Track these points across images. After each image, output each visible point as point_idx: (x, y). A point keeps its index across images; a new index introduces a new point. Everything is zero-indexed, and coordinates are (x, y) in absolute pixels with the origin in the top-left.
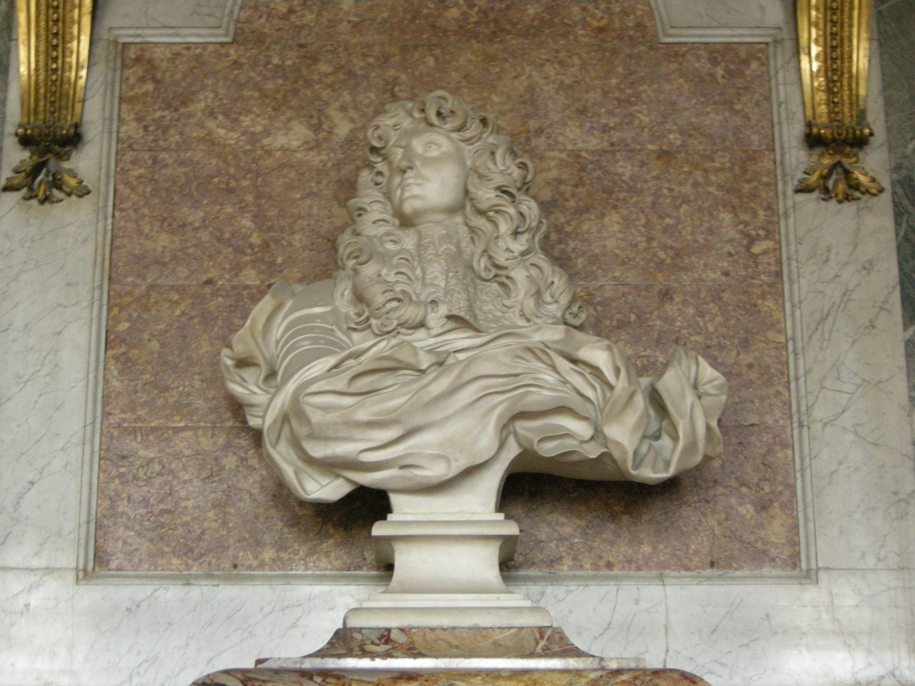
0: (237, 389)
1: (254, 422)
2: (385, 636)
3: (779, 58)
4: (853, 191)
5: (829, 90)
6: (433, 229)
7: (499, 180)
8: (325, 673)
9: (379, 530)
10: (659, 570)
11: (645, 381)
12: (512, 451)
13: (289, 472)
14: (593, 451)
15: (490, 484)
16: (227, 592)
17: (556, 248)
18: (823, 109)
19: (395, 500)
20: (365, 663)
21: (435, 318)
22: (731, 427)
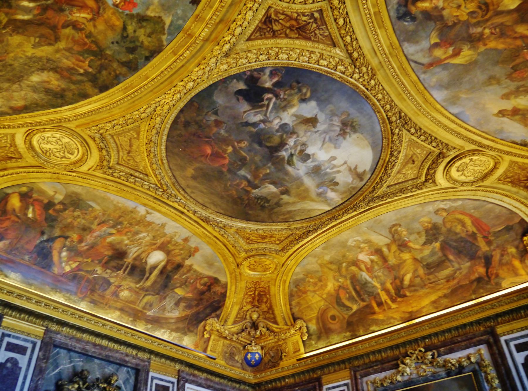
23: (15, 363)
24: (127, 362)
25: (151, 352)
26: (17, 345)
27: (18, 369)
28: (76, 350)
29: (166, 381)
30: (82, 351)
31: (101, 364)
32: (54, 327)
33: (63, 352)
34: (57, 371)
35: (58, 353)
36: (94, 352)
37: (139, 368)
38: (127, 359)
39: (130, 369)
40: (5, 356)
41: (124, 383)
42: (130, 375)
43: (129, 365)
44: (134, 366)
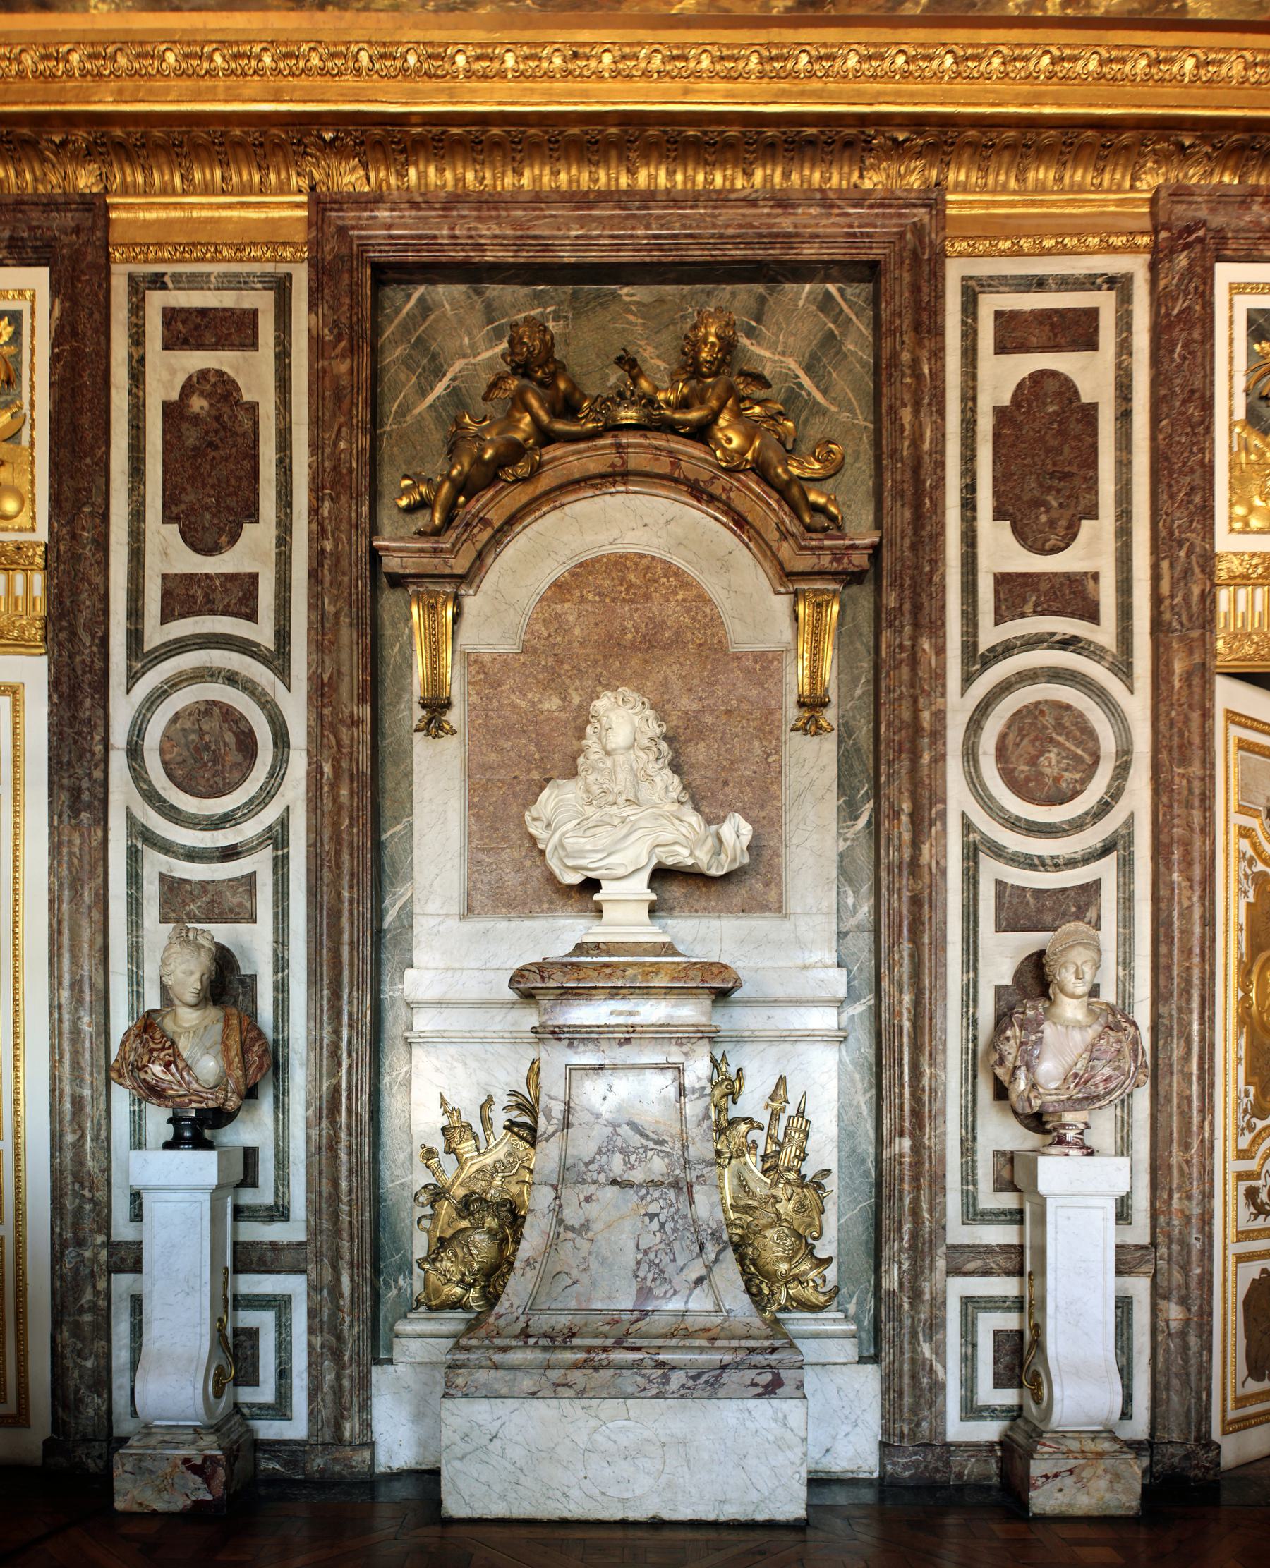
0: (531, 830)
1: (541, 846)
2: (597, 945)
3: (788, 660)
4: (819, 730)
5: (811, 677)
6: (620, 758)
7: (651, 735)
8: (572, 964)
9: (597, 897)
10: (719, 912)
11: (713, 828)
12: (654, 861)
13: (557, 871)
14: (690, 862)
15: (645, 876)
16: (528, 924)
17: (676, 767)
18: (807, 687)
19: (603, 883)
20: (589, 959)
21: (621, 800)
22: (754, 848)
23: (221, 389)
24: (788, 239)
25: (941, 137)
26: (203, 312)
27: (241, 414)
28: (490, 256)
29: (1067, 283)
30: (524, 256)
31: (661, 301)
32: (350, 178)
33: (447, 294)
34: (440, 388)
35: (425, 308)
36: (584, 243)
37: (876, 253)
38: (786, 223)
39: (831, 288)
40: (173, 372)
41: (809, 369)
42: (838, 317)
43: (809, 252)
44: (838, 253)
